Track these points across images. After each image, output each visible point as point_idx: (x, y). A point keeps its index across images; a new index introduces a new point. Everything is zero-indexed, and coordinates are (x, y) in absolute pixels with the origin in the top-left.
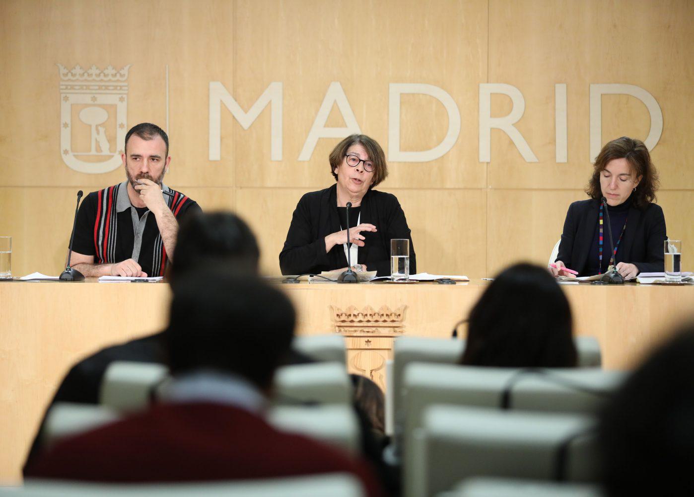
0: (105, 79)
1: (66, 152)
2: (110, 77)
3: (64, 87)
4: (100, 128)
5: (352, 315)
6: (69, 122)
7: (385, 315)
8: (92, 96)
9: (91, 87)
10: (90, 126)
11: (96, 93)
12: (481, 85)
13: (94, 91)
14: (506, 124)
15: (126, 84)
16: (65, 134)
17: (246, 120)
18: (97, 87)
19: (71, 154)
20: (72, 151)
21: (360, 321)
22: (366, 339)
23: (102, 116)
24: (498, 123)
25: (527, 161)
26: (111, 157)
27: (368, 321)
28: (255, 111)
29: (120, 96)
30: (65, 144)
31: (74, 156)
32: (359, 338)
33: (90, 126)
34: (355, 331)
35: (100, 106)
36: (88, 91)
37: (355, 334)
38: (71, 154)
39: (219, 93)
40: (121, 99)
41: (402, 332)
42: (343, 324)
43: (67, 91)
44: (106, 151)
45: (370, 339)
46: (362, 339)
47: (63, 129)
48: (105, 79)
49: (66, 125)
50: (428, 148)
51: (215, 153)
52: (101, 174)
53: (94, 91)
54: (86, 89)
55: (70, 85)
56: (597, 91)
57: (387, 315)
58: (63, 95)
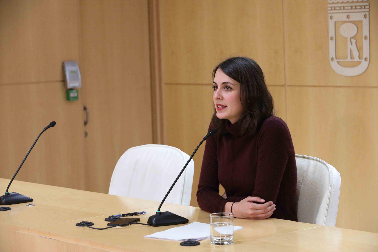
1: (332, 59)
3: (330, 8)
4: (352, 40)
6: (334, 36)
8: (347, 14)
9: (346, 8)
10: (347, 38)
11: (350, 12)
13: (348, 11)
15: (368, 4)
16: (332, 44)
18: (350, 8)
19: (335, 61)
20: (336, 59)
26: (360, 62)
29: (364, 13)
30: (332, 54)
31: (338, 62)
33: (347, 38)
36: (344, 11)
38: (335, 61)
40: (365, 16)
43: (332, 11)
44: (357, 59)
47: (330, 41)
49: (332, 38)
52: (355, 76)
53: (348, 11)
54: (344, 9)
55: (335, 7)
58: (330, 15)
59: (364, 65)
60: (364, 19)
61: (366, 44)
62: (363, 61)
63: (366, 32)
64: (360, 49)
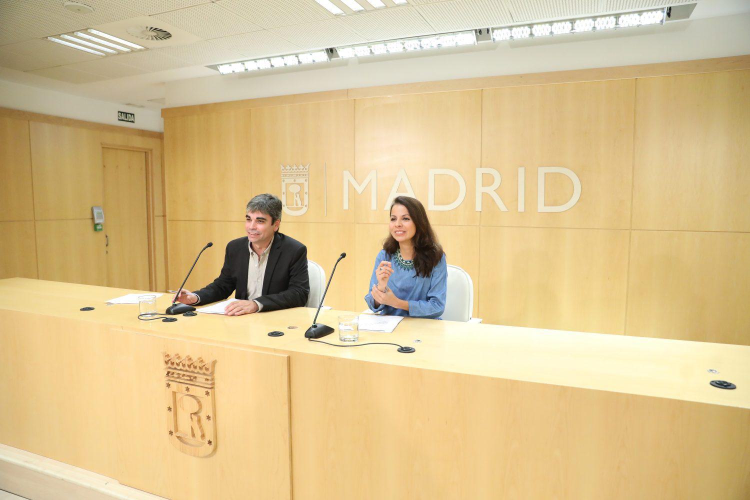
0: (299, 171)
2: (301, 170)
5: (175, 363)
6: (285, 192)
7: (198, 368)
12: (477, 169)
14: (490, 190)
17: (360, 189)
21: (181, 370)
22: (186, 386)
23: (296, 189)
24: (487, 190)
25: (502, 210)
26: (302, 208)
27: (187, 371)
28: (364, 185)
32: (181, 384)
33: (293, 193)
34: (179, 378)
35: (297, 184)
37: (178, 380)
39: (347, 176)
40: (306, 180)
41: (213, 384)
42: (171, 370)
44: (300, 206)
45: (189, 386)
46: (183, 385)
48: (299, 171)
50: (448, 204)
51: (346, 207)
56: (542, 171)
57: (200, 367)
59: (305, 209)
60: (305, 182)
61: (306, 197)
62: (304, 207)
63: (306, 190)
64: (302, 200)
